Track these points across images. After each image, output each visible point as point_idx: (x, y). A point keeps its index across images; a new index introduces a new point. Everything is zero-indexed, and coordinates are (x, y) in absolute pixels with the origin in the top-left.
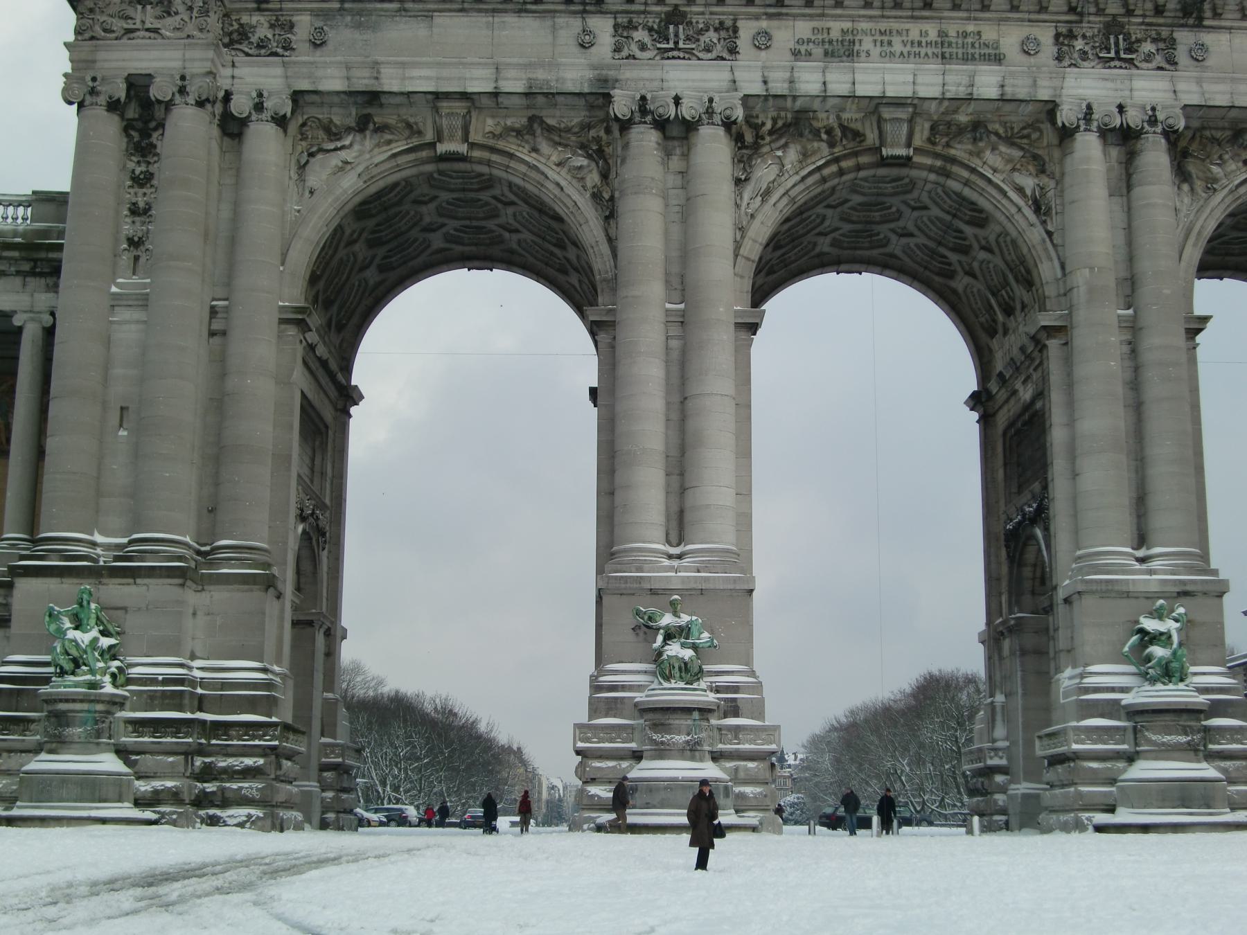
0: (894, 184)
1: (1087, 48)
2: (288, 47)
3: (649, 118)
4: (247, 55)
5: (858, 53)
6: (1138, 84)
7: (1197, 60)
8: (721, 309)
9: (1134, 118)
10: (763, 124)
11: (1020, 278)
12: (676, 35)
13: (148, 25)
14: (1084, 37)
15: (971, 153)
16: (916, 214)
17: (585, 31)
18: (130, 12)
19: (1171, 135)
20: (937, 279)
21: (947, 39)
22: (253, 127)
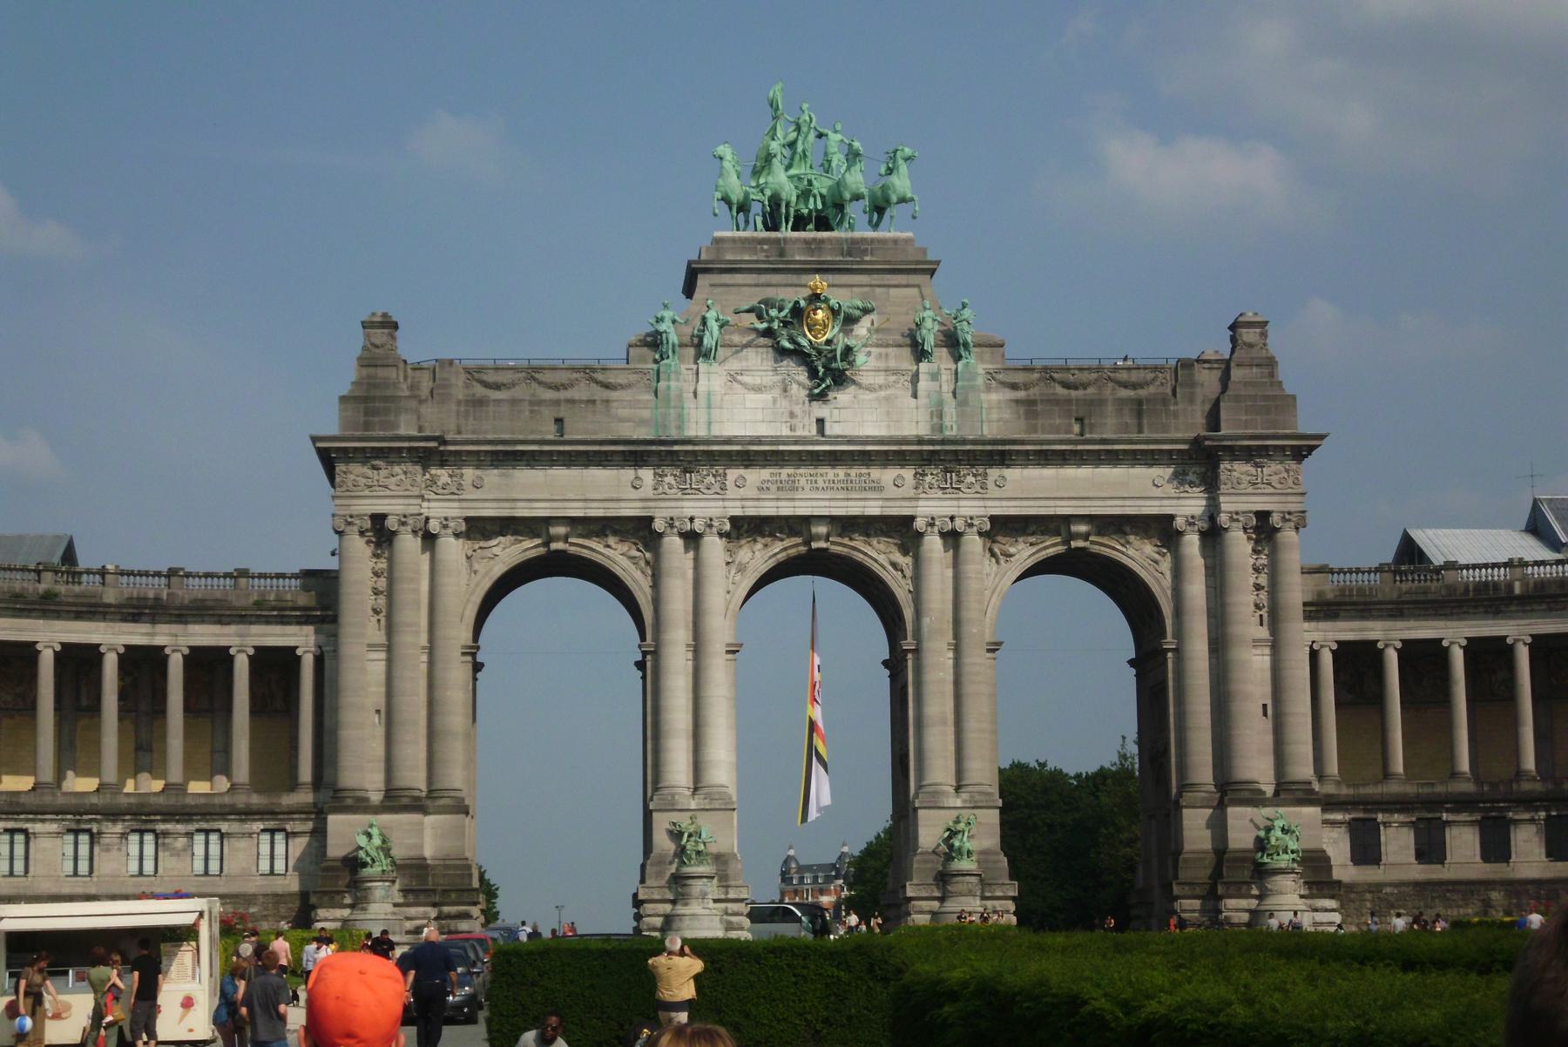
1: (934, 481)
2: (460, 487)
3: (676, 530)
4: (437, 494)
5: (797, 488)
6: (962, 503)
7: (1000, 487)
9: (959, 525)
10: (742, 526)
12: (691, 480)
13: (381, 484)
14: (932, 474)
17: (637, 478)
18: (369, 472)
21: (849, 478)
22: (442, 541)
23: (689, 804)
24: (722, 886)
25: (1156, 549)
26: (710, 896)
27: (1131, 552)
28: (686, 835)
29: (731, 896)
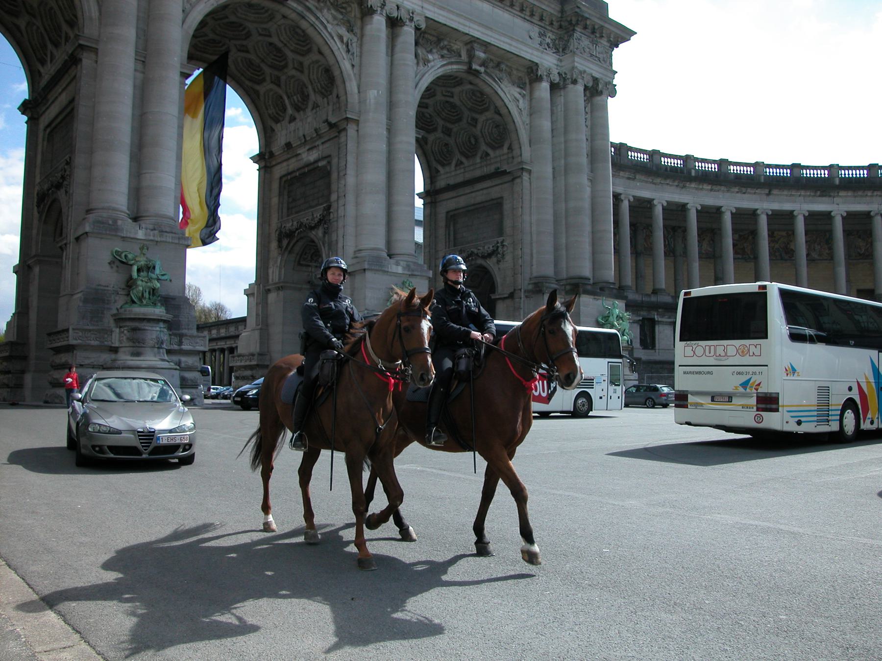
0: (257, 16)
8: (176, 59)
11: (317, 90)
15: (317, 8)
16: (260, 38)
19: (417, 29)
20: (247, 83)
23: (136, 233)
24: (175, 335)
25: (518, 90)
26: (164, 346)
27: (502, 86)
28: (135, 268)
29: (186, 347)
